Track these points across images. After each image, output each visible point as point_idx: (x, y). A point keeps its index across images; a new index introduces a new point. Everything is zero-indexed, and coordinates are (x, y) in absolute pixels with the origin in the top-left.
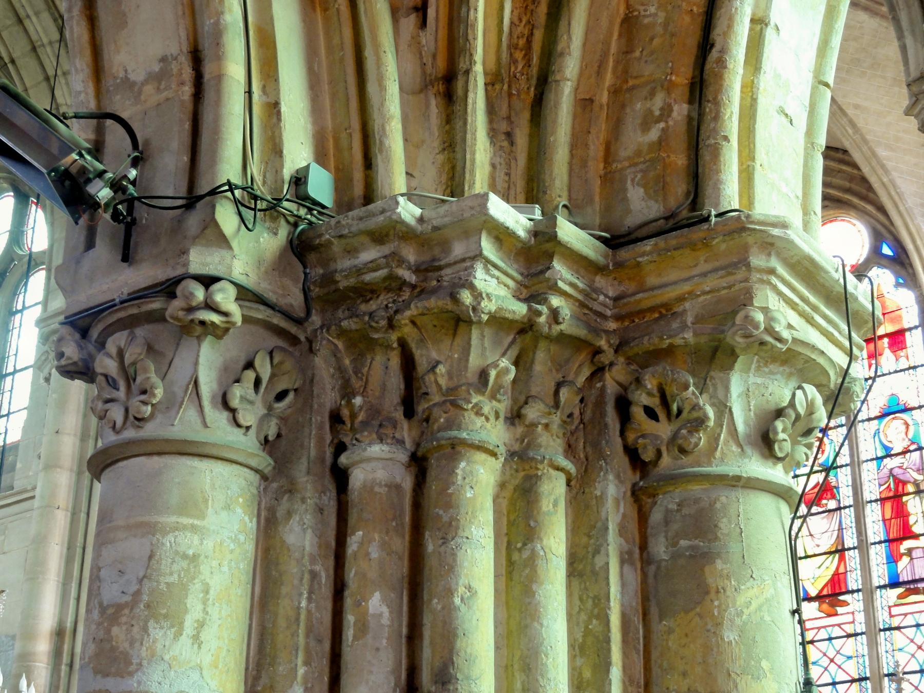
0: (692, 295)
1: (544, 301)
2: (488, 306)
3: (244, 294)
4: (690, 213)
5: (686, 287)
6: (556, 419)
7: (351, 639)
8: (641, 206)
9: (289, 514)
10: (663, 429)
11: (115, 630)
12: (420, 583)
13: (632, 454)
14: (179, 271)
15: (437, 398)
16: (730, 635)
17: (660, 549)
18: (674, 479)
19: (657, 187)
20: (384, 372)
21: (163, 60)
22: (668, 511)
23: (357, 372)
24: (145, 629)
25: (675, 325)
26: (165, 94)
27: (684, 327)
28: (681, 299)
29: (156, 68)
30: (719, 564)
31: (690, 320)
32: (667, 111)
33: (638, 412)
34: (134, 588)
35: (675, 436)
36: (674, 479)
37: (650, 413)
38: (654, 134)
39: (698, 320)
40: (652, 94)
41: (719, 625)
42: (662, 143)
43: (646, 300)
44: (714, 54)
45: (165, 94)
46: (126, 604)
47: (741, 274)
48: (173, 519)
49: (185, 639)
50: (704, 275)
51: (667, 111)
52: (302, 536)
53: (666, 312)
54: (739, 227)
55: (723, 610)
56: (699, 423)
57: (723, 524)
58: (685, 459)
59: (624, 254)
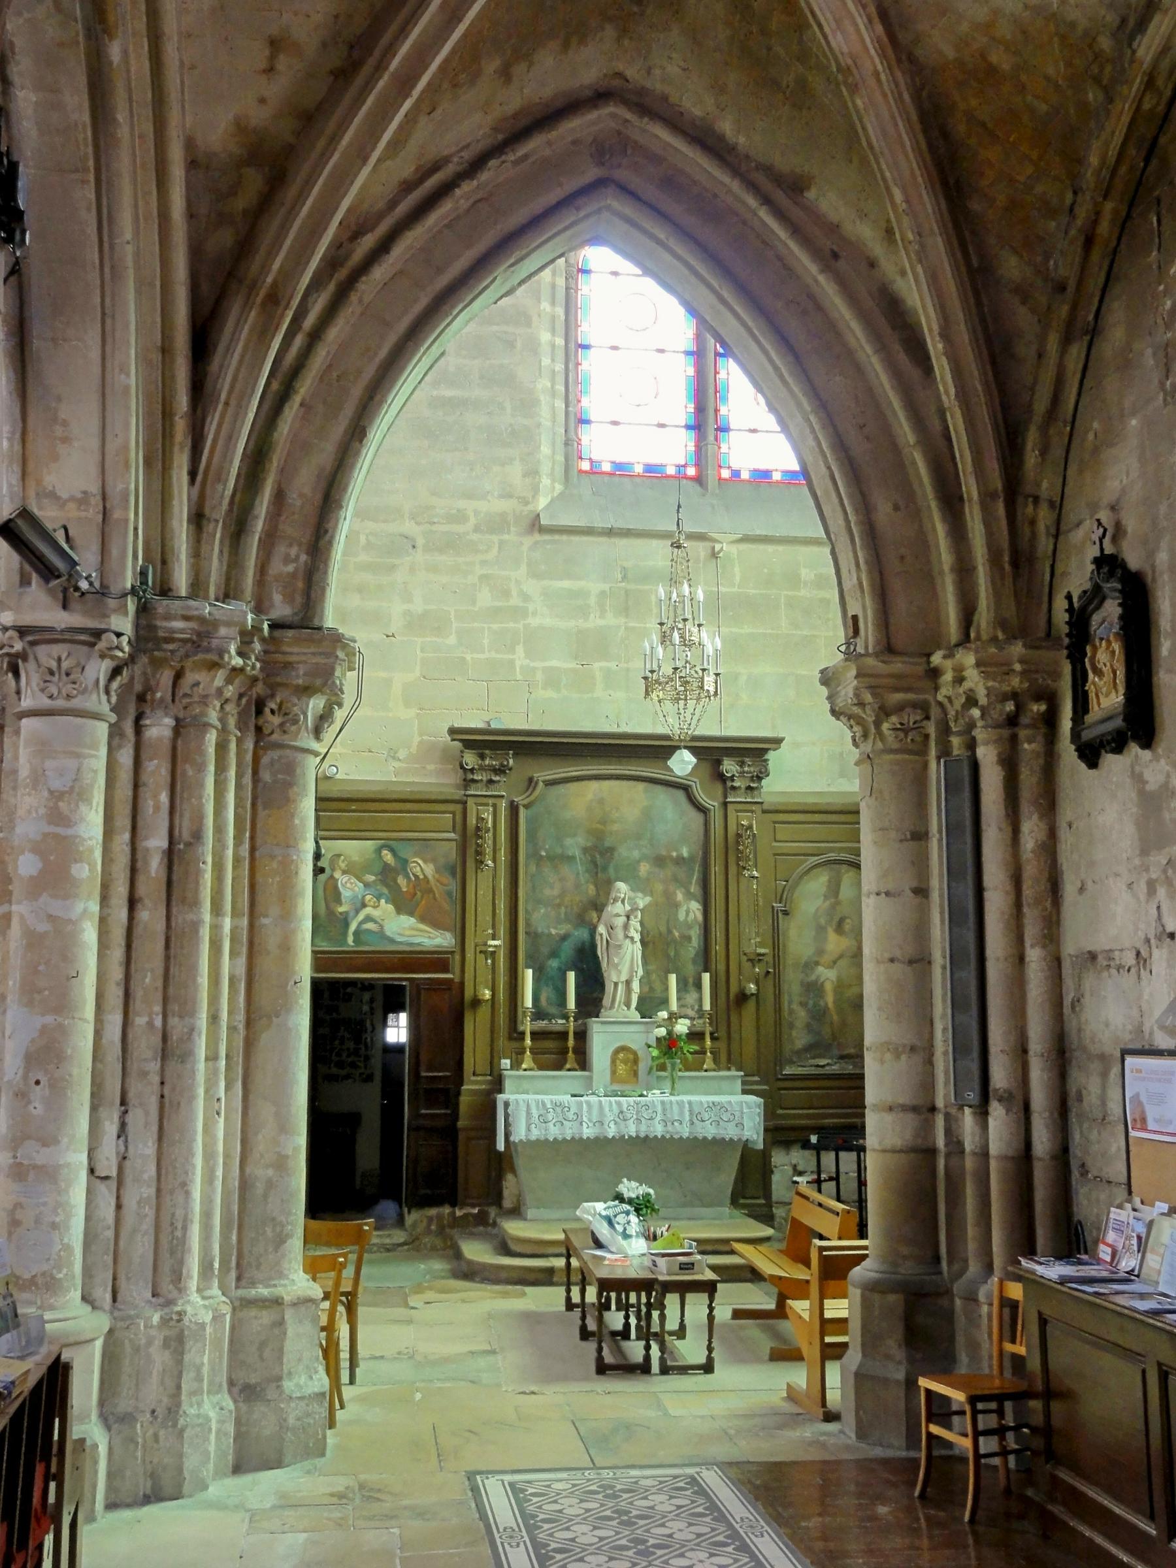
0: (305, 662)
1: (249, 658)
2: (233, 662)
3: (129, 642)
4: (305, 620)
5: (303, 658)
6: (235, 712)
7: (151, 811)
8: (281, 609)
9: (120, 747)
10: (276, 720)
11: (61, 804)
12: (178, 787)
13: (259, 729)
14: (103, 626)
15: (196, 699)
16: (297, 822)
17: (266, 776)
18: (281, 746)
19: (289, 599)
20: (166, 677)
21: (85, 493)
22: (272, 759)
23: (154, 676)
24: (77, 806)
25: (294, 673)
26: (83, 514)
27: (298, 677)
28: (298, 663)
29: (80, 496)
30: (295, 789)
31: (301, 673)
32: (297, 557)
33: (267, 710)
34: (70, 784)
35: (282, 725)
36: (281, 746)
37: (273, 712)
38: (290, 568)
39: (305, 675)
40: (291, 545)
41: (293, 816)
42: (294, 575)
43: (279, 657)
44: (327, 538)
45: (83, 514)
46: (66, 792)
47: (332, 660)
48: (87, 751)
49: (93, 811)
50: (313, 654)
51: (297, 557)
52: (126, 757)
53: (288, 666)
54: (336, 639)
55: (296, 808)
56: (295, 722)
57: (298, 771)
58: (286, 737)
59: (278, 633)
